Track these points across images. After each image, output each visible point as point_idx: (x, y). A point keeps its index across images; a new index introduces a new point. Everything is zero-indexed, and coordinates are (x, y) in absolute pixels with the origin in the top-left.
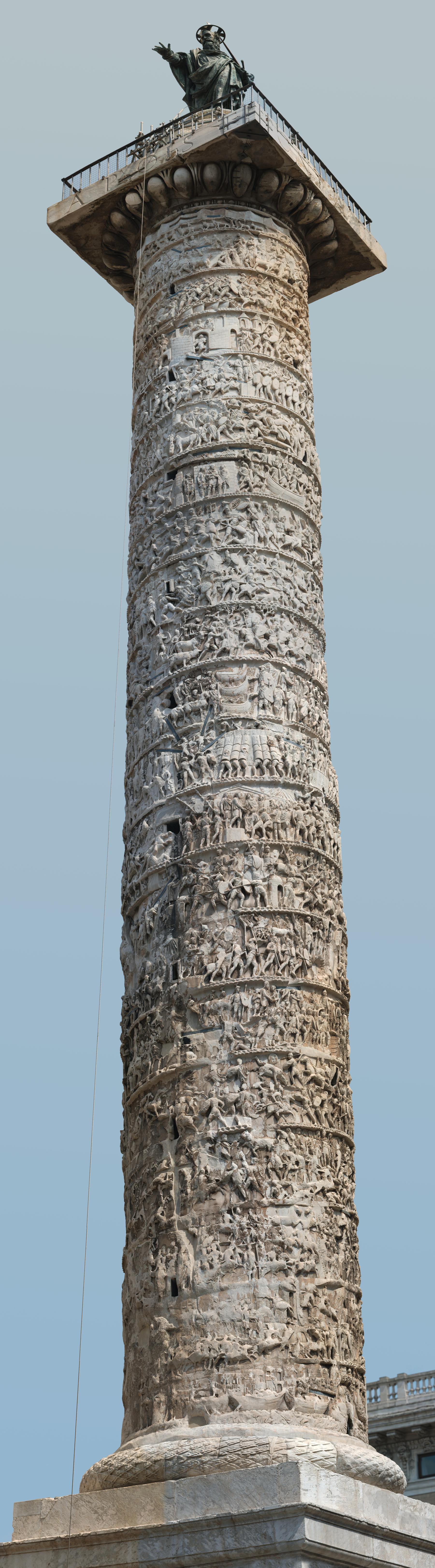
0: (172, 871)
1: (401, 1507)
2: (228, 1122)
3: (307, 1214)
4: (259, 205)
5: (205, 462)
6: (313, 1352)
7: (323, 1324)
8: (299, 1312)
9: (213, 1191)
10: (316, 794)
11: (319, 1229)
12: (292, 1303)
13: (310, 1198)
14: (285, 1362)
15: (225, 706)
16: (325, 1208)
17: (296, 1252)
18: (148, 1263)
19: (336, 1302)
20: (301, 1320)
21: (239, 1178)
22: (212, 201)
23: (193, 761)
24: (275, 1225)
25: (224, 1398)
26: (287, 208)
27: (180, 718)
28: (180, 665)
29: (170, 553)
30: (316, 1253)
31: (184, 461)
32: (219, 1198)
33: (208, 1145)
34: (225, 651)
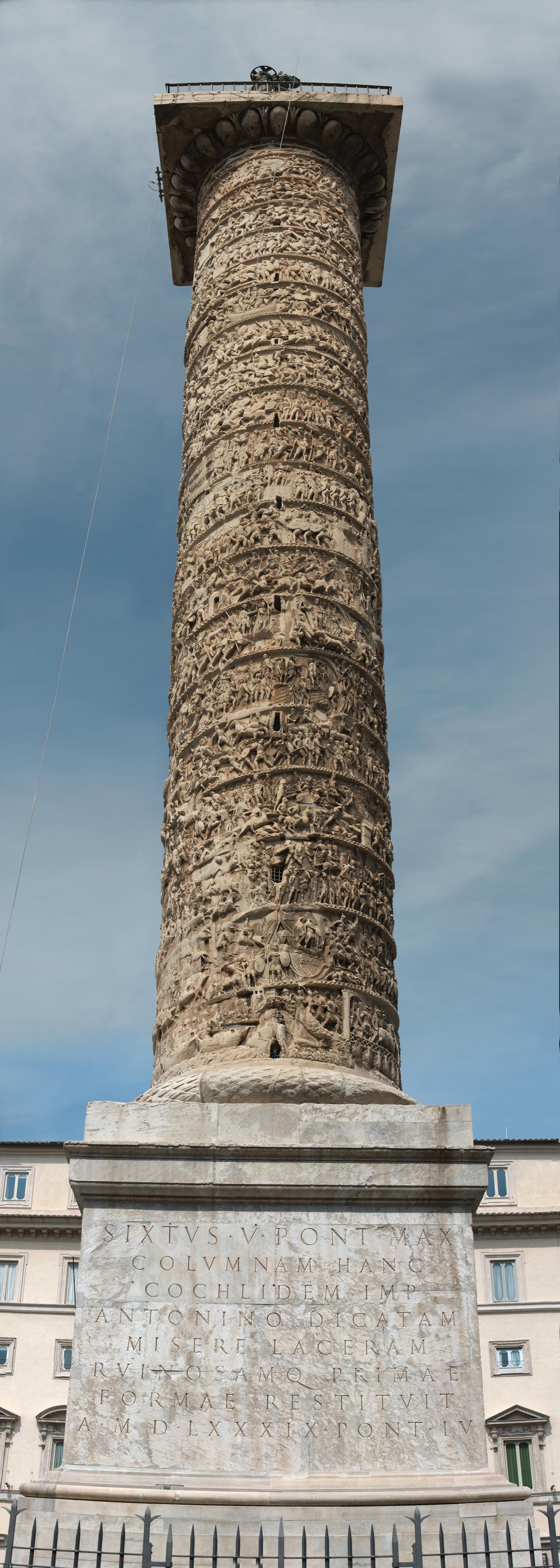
1: (305, 1117)
3: (228, 859)
6: (227, 988)
7: (241, 956)
8: (214, 954)
10: (266, 505)
11: (244, 867)
12: (208, 951)
13: (232, 843)
14: (199, 1009)
16: (252, 844)
17: (215, 899)
19: (265, 928)
20: (215, 961)
24: (199, 884)
30: (233, 891)
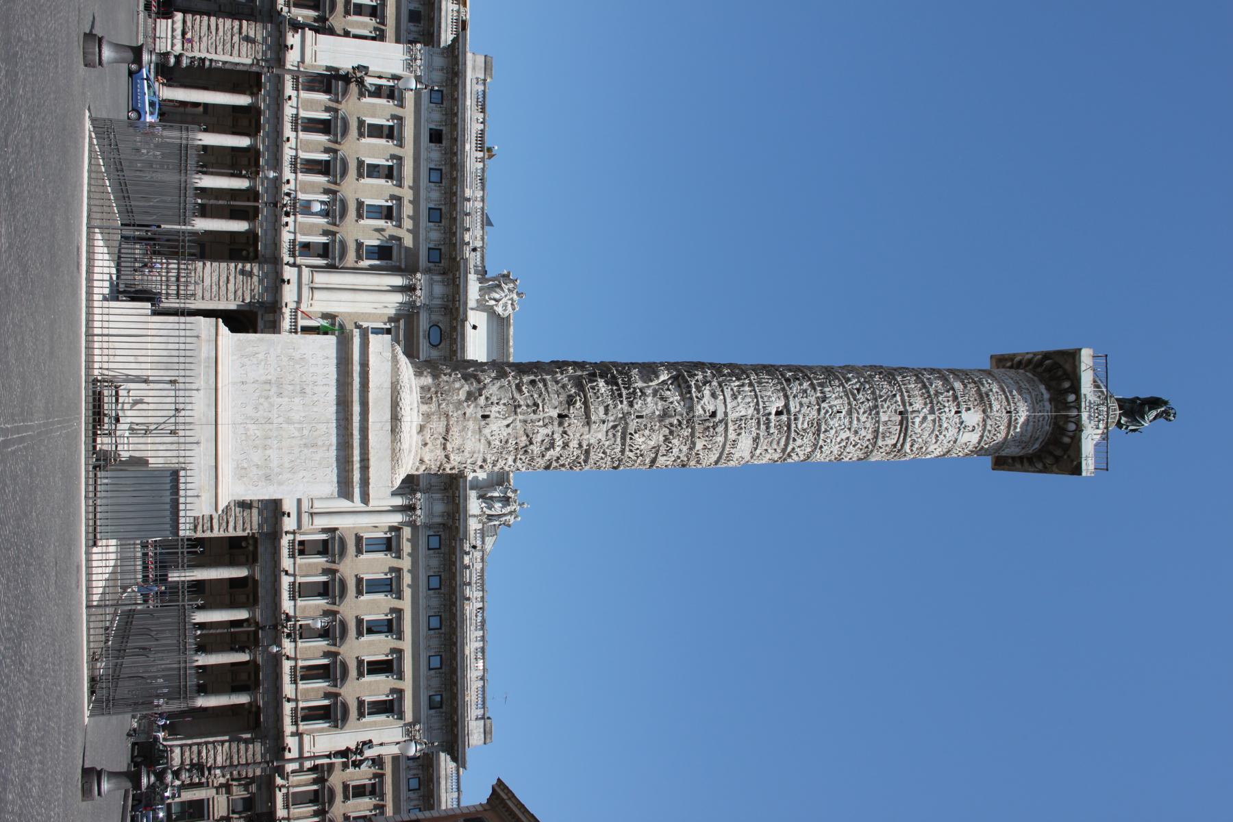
0: (691, 415)
2: (560, 443)
4: (1040, 450)
5: (901, 431)
9: (528, 436)
15: (766, 441)
18: (500, 399)
21: (531, 447)
22: (1051, 434)
23: (743, 425)
25: (428, 441)
26: (1034, 460)
27: (767, 419)
28: (796, 419)
29: (858, 413)
31: (905, 422)
32: (524, 438)
33: (550, 434)
34: (794, 440)
